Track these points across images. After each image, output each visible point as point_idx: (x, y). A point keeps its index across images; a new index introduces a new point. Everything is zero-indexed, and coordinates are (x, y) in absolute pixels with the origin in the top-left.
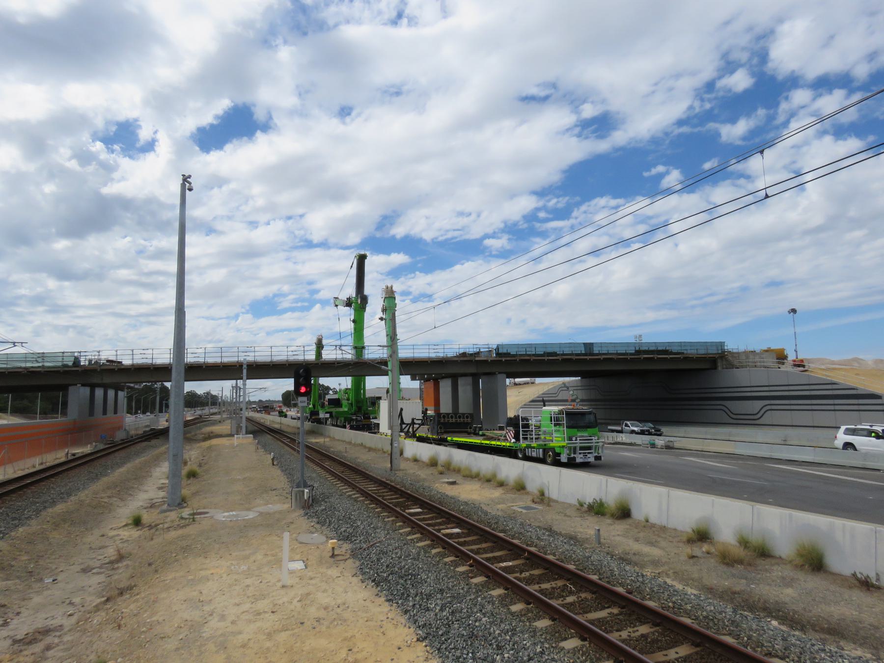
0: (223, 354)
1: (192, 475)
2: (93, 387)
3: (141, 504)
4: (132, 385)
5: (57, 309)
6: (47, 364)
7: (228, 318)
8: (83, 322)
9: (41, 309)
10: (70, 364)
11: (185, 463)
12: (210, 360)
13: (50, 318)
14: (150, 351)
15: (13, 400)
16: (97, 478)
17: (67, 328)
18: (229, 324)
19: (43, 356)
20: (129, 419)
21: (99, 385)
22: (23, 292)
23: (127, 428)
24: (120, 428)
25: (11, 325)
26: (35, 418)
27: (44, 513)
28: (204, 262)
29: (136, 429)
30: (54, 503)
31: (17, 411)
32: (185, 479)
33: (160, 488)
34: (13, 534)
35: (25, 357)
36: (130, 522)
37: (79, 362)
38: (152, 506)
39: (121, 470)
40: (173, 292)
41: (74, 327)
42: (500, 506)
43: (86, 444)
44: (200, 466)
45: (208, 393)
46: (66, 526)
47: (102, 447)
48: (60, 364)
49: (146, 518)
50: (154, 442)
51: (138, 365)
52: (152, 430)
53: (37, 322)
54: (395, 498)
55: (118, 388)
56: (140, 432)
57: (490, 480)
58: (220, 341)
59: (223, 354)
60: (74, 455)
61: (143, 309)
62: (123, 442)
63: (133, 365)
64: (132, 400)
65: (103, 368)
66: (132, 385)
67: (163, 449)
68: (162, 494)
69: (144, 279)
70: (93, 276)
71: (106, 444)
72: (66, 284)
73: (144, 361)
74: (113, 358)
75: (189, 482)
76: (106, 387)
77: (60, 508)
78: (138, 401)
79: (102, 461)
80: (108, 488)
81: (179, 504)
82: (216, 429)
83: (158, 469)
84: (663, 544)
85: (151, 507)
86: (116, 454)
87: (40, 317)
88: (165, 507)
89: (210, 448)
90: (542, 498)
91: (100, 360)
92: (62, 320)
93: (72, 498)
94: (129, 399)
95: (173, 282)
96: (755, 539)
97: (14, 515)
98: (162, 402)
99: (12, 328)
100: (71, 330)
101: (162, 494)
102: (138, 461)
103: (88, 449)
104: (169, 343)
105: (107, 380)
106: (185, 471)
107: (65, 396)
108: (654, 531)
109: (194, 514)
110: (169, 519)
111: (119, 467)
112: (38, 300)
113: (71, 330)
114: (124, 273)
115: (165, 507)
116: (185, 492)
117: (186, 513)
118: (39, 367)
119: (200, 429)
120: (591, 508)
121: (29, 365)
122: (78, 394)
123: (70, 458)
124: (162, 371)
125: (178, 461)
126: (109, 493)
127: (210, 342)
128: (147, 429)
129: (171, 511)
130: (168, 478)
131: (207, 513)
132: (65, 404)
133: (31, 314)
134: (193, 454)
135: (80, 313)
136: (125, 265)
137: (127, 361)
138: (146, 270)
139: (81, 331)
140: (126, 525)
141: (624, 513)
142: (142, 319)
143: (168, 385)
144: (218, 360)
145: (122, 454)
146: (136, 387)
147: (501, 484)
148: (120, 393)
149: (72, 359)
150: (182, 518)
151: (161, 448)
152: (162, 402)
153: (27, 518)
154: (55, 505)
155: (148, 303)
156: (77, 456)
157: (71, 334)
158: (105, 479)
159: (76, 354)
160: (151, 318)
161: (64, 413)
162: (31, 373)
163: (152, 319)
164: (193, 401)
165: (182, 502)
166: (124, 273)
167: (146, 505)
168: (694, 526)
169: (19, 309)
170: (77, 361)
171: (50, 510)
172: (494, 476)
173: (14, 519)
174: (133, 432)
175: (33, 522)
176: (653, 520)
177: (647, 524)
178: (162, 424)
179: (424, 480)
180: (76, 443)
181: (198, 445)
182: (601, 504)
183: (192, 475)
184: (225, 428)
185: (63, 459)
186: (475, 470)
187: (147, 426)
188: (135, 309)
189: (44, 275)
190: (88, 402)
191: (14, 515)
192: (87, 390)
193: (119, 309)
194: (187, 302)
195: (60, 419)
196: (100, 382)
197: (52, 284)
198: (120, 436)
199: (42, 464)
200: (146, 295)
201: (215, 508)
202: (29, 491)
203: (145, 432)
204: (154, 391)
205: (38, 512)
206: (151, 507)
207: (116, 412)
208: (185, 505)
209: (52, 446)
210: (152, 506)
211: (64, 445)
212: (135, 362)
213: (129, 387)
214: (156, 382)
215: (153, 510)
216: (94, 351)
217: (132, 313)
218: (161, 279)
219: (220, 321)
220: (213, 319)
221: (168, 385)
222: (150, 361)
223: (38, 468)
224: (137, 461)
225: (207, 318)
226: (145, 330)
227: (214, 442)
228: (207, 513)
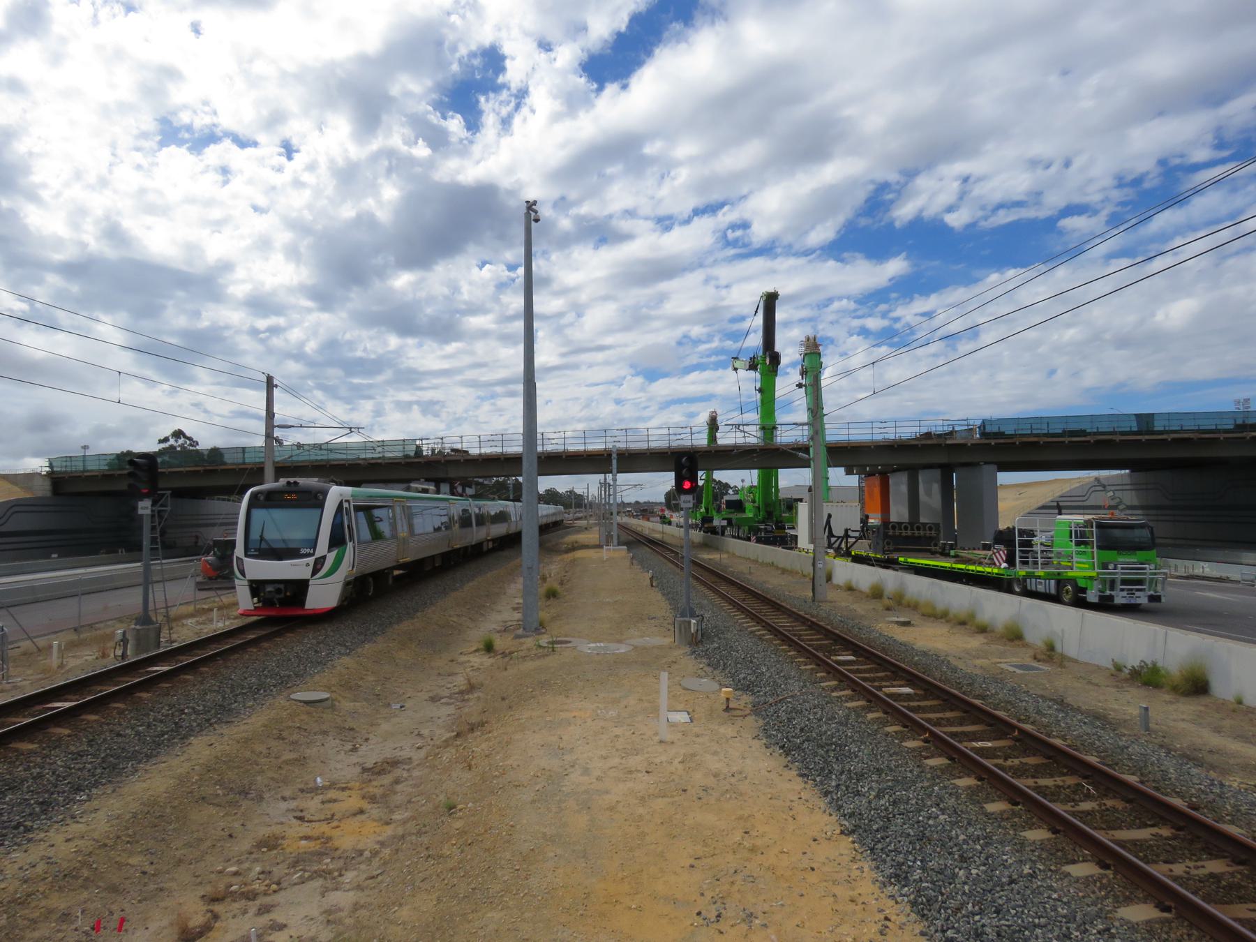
0: (608, 439)
1: (552, 594)
3: (494, 626)
10: (412, 454)
21: (444, 480)
33: (514, 609)
35: (365, 447)
48: (400, 455)
51: (486, 454)
59: (608, 439)
63: (480, 455)
68: (517, 616)
74: (459, 446)
82: (582, 538)
83: (513, 586)
89: (573, 561)
101: (517, 616)
105: (453, 473)
121: (369, 456)
134: (554, 567)
137: (474, 451)
143: (520, 479)
144: (581, 448)
170: (419, 450)
172: (972, 616)
181: (560, 558)
183: (552, 594)
184: (592, 537)
186: (940, 607)
213: (477, 484)
214: (508, 476)
221: (520, 479)
227: (579, 554)
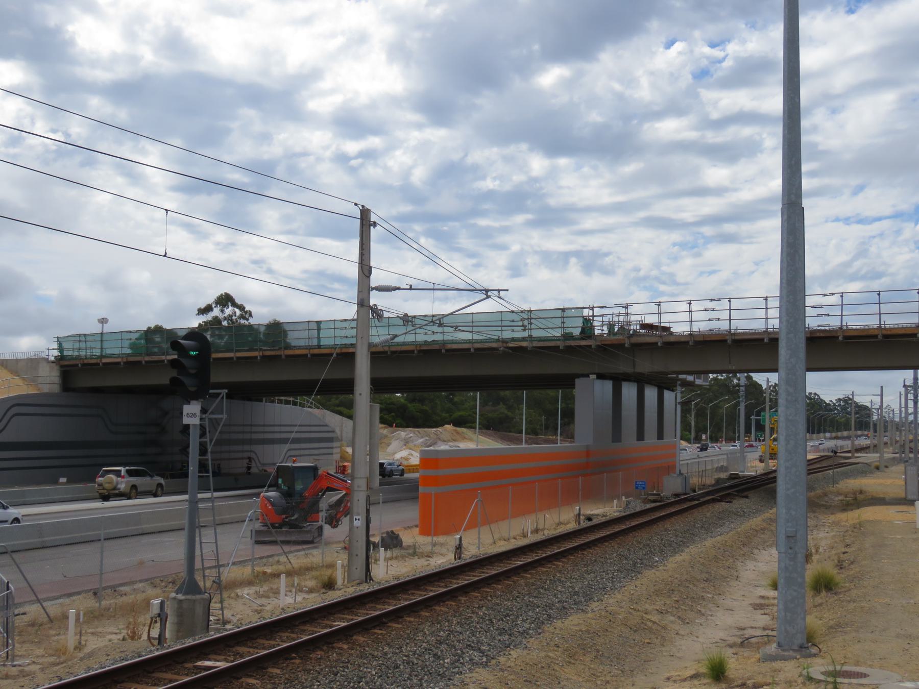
1: (824, 585)
2: (618, 380)
3: (722, 635)
4: (690, 378)
5: (551, 217)
6: (536, 334)
7: (897, 216)
8: (594, 243)
9: (520, 219)
10: (577, 332)
11: (808, 557)
12: (855, 322)
13: (538, 239)
14: (725, 304)
15: (484, 404)
16: (634, 570)
17: (566, 256)
18: (899, 232)
19: (529, 317)
20: (688, 453)
21: (628, 378)
22: (489, 184)
23: (684, 471)
24: (670, 469)
25: (472, 255)
26: (520, 441)
27: (548, 628)
28: (842, 80)
29: (702, 474)
30: (564, 612)
31: (495, 425)
32: (809, 593)
33: (757, 607)
34: (502, 659)
35: (501, 320)
36: (703, 670)
37: (592, 328)
38: (744, 643)
39: (678, 558)
40: (773, 161)
41: (578, 254)
43: (611, 498)
44: (840, 566)
45: (848, 401)
46: (588, 659)
47: (638, 506)
48: (558, 333)
49: (736, 667)
50: (739, 504)
51: (701, 334)
52: (733, 477)
53: (516, 248)
55: (664, 383)
56: (709, 481)
58: (878, 275)
60: (589, 519)
61: (711, 206)
62: (679, 499)
63: (691, 335)
64: (689, 411)
65: (635, 340)
66: (690, 378)
67: (756, 521)
68: (762, 620)
69: (712, 137)
70: (610, 144)
71: (646, 501)
72: (563, 161)
73: (715, 325)
74: (652, 320)
75: (818, 600)
76: (641, 381)
77: (574, 622)
78: (700, 414)
79: (643, 536)
80: (658, 593)
81: (801, 647)
82: (871, 484)
83: (750, 565)
85: (742, 644)
86: (668, 524)
87: (524, 238)
88: (772, 648)
89: (858, 527)
91: (629, 323)
92: (558, 241)
93: (594, 605)
94: (685, 405)
95: (772, 141)
97: (501, 624)
98: (750, 415)
99: (474, 261)
100: (573, 260)
101: (762, 620)
102: (708, 544)
103: (610, 509)
104: (768, 280)
105: (645, 366)
106: (811, 571)
107: (570, 399)
109: (836, 674)
110: (781, 677)
111: (675, 552)
112: (515, 200)
113: (573, 260)
114: (669, 128)
115: (772, 648)
116: (812, 621)
117: (818, 668)
118: (524, 339)
119: (835, 482)
121: (507, 334)
122: (593, 394)
123: (585, 524)
124: (758, 348)
125: (796, 551)
126: (659, 604)
127: (853, 278)
128: (724, 475)
129: (785, 659)
130: (775, 586)
131: (865, 676)
132: (569, 415)
133: (505, 230)
134: (824, 536)
135: (589, 223)
136: (673, 109)
137: (680, 328)
138: (715, 115)
139: (592, 262)
140: (695, 676)
142: (708, 230)
143: (761, 378)
144: (872, 322)
145: (678, 525)
146: (699, 382)
148: (668, 396)
149: (579, 323)
150: (810, 679)
151: (753, 518)
152: (750, 415)
153: (521, 634)
154: (566, 616)
155: (718, 191)
156: (595, 521)
157: (574, 269)
158: (650, 574)
159: (586, 312)
160: (726, 225)
161: (569, 436)
162: (515, 352)
163: (729, 228)
164: (821, 417)
165: (808, 645)
166: (669, 128)
167: (732, 640)
169: (483, 222)
170: (587, 324)
171: (559, 624)
173: (502, 632)
174: (695, 481)
175: (533, 642)
178: (753, 466)
180: (591, 494)
181: (832, 518)
183: (824, 585)
184: (891, 482)
185: (572, 526)
187: (722, 469)
188: (692, 209)
189: (524, 146)
190: (610, 412)
191: (501, 624)
192: (608, 385)
193: (661, 209)
194: (807, 184)
195: (561, 445)
196: (629, 370)
197: (538, 164)
198: (671, 486)
199: (536, 531)
200: (716, 174)
201: (881, 667)
202: (522, 582)
203: (718, 481)
204: (733, 392)
205: (539, 624)
206: (742, 644)
207: (660, 436)
208: (814, 650)
209: (554, 498)
210: (744, 643)
211: (570, 496)
212: (695, 329)
213: (685, 384)
214: (734, 372)
215: (746, 652)
216: (617, 306)
217: (687, 216)
218: (747, 131)
219: (876, 227)
220: (862, 221)
221: (761, 378)
222: (724, 326)
223: (532, 539)
224: (709, 542)
225: (847, 221)
226: (715, 253)
227: (868, 513)
228: (865, 676)
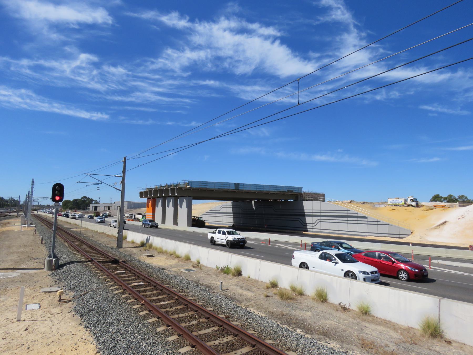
42: (174, 269)
54: (113, 264)
57: (173, 255)
84: (254, 289)
90: (198, 265)
96: (298, 287)
108: (252, 284)
120: (222, 270)
141: (239, 273)
147: (178, 257)
168: (271, 280)
172: (175, 253)
176: (252, 277)
177: (249, 279)
179: (135, 254)
182: (228, 269)
186: (164, 249)
